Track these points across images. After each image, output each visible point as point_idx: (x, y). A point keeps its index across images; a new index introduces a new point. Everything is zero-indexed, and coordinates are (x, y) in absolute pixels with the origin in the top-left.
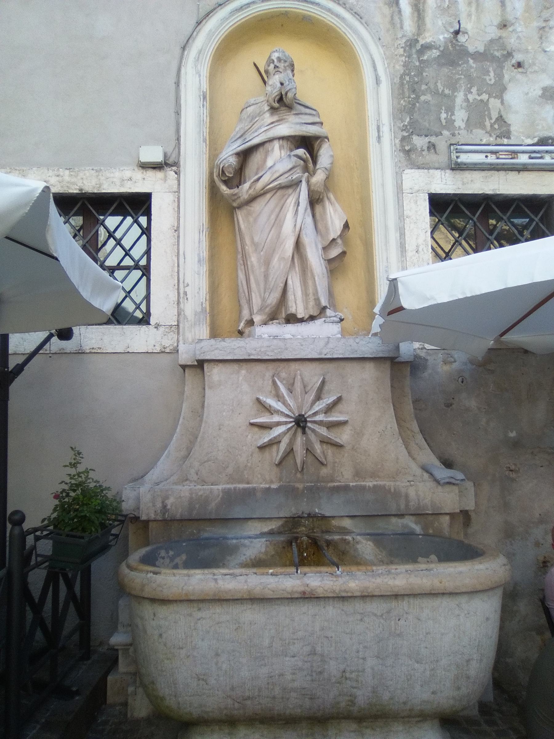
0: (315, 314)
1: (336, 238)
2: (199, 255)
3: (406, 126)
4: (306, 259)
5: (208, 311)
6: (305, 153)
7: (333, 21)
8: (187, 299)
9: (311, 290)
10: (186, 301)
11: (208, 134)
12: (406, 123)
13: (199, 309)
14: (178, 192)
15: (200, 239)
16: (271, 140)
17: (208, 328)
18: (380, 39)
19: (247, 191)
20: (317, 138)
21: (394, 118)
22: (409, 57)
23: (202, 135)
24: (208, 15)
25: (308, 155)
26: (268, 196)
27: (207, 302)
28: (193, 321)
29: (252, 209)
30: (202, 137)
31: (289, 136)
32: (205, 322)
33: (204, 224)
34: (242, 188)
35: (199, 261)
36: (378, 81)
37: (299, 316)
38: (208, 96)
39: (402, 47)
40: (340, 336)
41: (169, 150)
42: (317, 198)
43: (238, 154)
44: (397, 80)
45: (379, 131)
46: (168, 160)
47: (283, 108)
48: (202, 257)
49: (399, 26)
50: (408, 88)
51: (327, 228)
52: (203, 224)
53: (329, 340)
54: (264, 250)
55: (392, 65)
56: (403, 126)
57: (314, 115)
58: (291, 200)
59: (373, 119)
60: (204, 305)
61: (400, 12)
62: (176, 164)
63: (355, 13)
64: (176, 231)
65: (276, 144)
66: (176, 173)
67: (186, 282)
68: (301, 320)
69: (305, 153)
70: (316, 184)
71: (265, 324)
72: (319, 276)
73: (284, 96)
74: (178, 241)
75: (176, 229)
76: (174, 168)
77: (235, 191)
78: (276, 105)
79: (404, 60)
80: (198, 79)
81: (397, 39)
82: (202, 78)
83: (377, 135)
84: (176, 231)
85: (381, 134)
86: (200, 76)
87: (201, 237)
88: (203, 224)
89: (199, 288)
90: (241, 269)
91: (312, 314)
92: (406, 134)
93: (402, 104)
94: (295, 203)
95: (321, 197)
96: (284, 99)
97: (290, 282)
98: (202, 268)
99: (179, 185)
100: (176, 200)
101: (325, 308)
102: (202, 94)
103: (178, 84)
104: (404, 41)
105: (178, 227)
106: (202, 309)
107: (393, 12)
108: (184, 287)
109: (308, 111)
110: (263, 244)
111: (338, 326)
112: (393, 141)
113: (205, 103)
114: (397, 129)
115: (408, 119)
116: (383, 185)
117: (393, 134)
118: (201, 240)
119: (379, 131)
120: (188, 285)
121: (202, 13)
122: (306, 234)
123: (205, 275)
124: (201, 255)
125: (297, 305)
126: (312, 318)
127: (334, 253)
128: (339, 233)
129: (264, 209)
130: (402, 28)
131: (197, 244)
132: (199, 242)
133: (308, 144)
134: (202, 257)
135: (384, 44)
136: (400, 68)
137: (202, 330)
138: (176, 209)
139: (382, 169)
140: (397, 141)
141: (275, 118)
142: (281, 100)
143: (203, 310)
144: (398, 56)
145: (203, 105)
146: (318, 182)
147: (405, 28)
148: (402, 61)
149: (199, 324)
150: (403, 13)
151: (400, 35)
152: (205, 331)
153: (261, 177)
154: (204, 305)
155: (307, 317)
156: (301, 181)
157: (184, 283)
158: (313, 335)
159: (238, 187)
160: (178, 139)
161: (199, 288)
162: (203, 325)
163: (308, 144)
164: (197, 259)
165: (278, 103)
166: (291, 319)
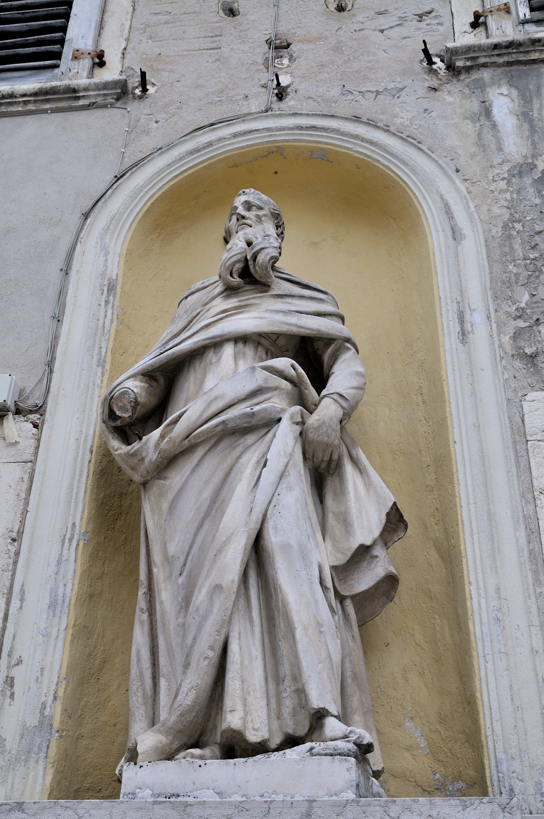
0: (302, 731)
1: (368, 543)
2: (54, 592)
3: (523, 309)
4: (277, 588)
5: (56, 725)
6: (293, 366)
7: (365, 151)
8: (12, 695)
9: (286, 669)
10: (8, 700)
11: (109, 351)
12: (523, 305)
13: (33, 721)
14: (33, 462)
15: (61, 555)
16: (216, 344)
17: (51, 772)
18: (458, 171)
19: (157, 445)
20: (329, 340)
21: (496, 297)
22: (519, 193)
23: (96, 351)
24: (137, 165)
25: (300, 370)
26: (200, 452)
27: (59, 703)
28: (14, 752)
29: (167, 482)
30: (95, 357)
31: (261, 335)
32: (42, 755)
33: (78, 524)
34: (148, 440)
35: (53, 605)
36: (456, 235)
37: (253, 737)
38: (119, 289)
39: (503, 179)
40: (351, 795)
41: (29, 385)
42: (326, 458)
43: (148, 375)
44: (497, 231)
45: (462, 322)
46: (23, 401)
47: (248, 287)
48: (60, 598)
49: (493, 147)
50: (523, 243)
51: (346, 522)
52: (74, 524)
53: (311, 808)
54: (185, 573)
55: (485, 208)
56: (517, 309)
57: (321, 300)
58: (250, 459)
59: (449, 299)
60: (48, 710)
61: (494, 126)
62: (40, 409)
63: (408, 136)
64: (14, 540)
65: (229, 350)
66: (36, 426)
67: (16, 656)
68: (261, 748)
69: (293, 366)
70: (320, 427)
71: (170, 757)
72: (305, 629)
73: (250, 263)
74: (15, 563)
75: (14, 535)
76: (34, 417)
77: (136, 445)
78: (236, 280)
79: (509, 198)
80: (102, 259)
81: (492, 166)
82: (110, 257)
83: (458, 328)
84: (14, 540)
85: (468, 326)
86: (107, 254)
87: (65, 552)
88: (74, 524)
89: (42, 669)
90: (142, 622)
91: (290, 731)
92: (521, 324)
93: (511, 272)
94: (258, 462)
95: (335, 457)
96: (251, 267)
97: (234, 648)
98: (56, 620)
99: (37, 448)
100: (26, 477)
101: (319, 716)
102: (106, 282)
103: (66, 271)
104: (506, 168)
105: (20, 533)
106: (41, 723)
107: (481, 130)
108: (9, 667)
109: (307, 292)
110: (182, 558)
111: (346, 765)
112: (496, 339)
113: (111, 298)
114: (503, 317)
115: (526, 297)
116: (477, 427)
117: (494, 326)
118: (64, 559)
119: (462, 322)
120: (19, 662)
121: (128, 162)
122: (275, 528)
123: (62, 635)
124: (61, 591)
125: (248, 711)
126: (291, 742)
127: (366, 580)
128: (376, 533)
129: (191, 482)
130: (500, 149)
131: (52, 568)
132: (59, 563)
133: (313, 356)
134: (60, 598)
135: (467, 177)
136: (500, 212)
137: (32, 774)
138: (23, 495)
139: (474, 393)
140: (506, 339)
141: (232, 302)
142: (246, 274)
143: (45, 723)
144: (496, 193)
145: (107, 302)
146: (324, 422)
147: (506, 149)
148: (506, 200)
149: (26, 761)
150: (500, 128)
151: (497, 160)
152: (40, 779)
153: (186, 411)
154: (47, 712)
155: (276, 740)
156: (279, 420)
157: (9, 656)
158: (274, 792)
159: (140, 439)
160: (50, 365)
161: (42, 669)
162: (37, 762)
163: (313, 356)
164: (47, 601)
165: (240, 277)
166: (235, 748)
